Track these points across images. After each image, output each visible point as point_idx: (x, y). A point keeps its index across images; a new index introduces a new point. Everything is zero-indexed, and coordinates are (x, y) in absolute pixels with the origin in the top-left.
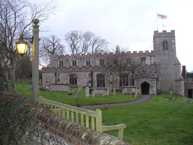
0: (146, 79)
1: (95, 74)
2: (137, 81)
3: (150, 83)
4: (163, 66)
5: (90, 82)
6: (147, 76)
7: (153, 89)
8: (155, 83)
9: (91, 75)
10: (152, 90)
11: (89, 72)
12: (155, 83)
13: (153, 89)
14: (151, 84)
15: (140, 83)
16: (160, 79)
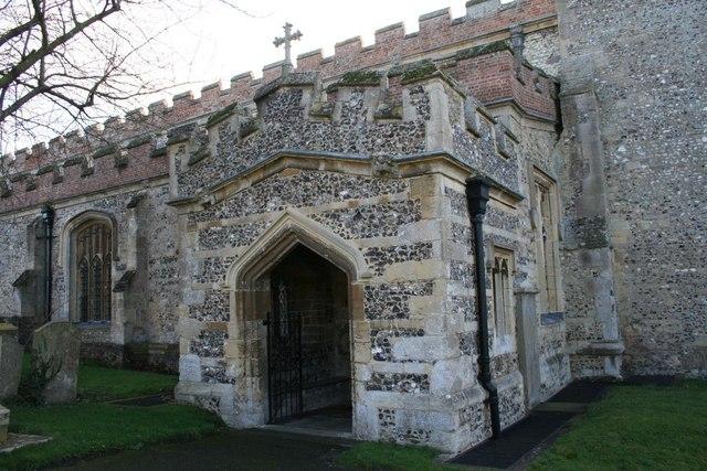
0: (306, 201)
1: (65, 216)
2: (206, 240)
3: (352, 249)
4: (646, 101)
5: (23, 282)
6: (318, 150)
7: (402, 347)
8: (422, 250)
9: (43, 234)
10: (387, 368)
11: (38, 213)
12: (422, 250)
13: (402, 347)
14: (362, 267)
15: (238, 255)
16: (619, 231)
